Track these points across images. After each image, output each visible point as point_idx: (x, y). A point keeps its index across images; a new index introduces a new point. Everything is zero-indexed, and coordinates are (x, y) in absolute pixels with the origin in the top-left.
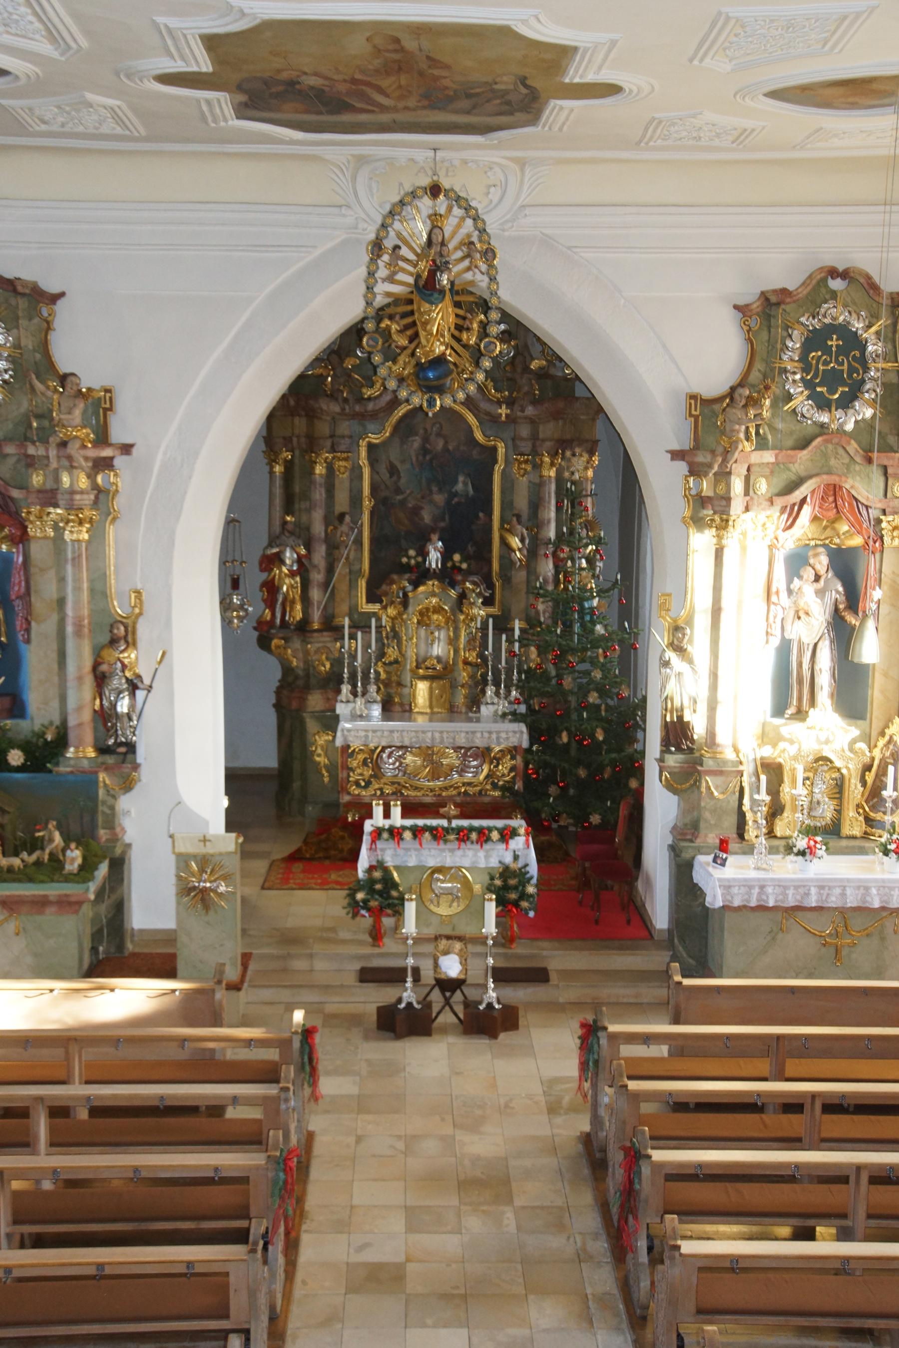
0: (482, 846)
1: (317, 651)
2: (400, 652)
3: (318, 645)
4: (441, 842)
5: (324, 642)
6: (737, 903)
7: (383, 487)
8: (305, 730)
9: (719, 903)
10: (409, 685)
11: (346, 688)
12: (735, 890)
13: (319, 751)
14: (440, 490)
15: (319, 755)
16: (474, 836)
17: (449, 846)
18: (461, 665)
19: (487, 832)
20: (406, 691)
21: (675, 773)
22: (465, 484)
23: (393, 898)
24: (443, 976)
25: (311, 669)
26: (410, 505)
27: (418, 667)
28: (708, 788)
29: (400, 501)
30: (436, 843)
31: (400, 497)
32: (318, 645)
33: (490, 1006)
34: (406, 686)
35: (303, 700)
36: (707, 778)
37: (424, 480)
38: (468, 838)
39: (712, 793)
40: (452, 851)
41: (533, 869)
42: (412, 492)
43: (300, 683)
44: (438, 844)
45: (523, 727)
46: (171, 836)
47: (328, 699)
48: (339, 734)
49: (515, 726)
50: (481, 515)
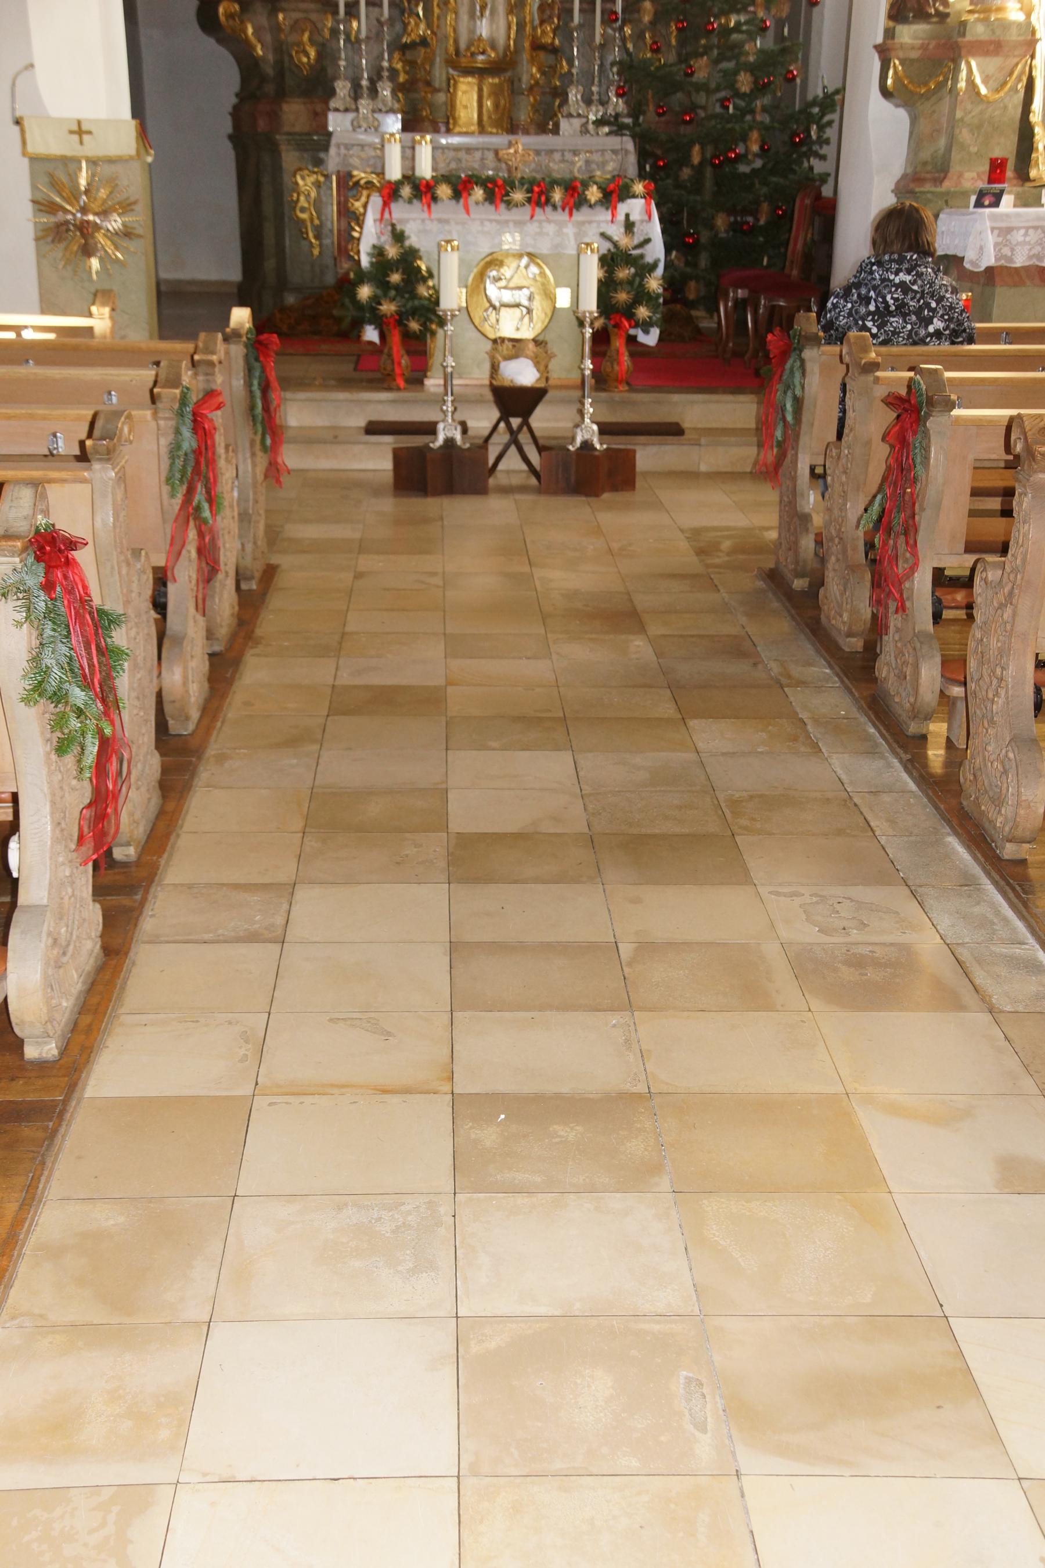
0: (571, 215)
1: (296, 27)
2: (429, 26)
3: (295, 15)
4: (502, 206)
5: (305, 11)
6: (1020, 261)
8: (281, 168)
9: (989, 260)
10: (444, 85)
11: (343, 88)
12: (1018, 236)
13: (303, 202)
15: (303, 210)
16: (557, 196)
17: (517, 214)
18: (525, 56)
19: (580, 189)
20: (441, 97)
21: (912, 61)
23: (421, 298)
24: (507, 384)
25: (286, 59)
27: (457, 52)
28: (970, 82)
30: (492, 208)
32: (295, 15)
33: (587, 445)
34: (439, 90)
35: (274, 116)
36: (973, 63)
38: (548, 201)
39: (978, 93)
40: (519, 224)
41: (656, 251)
43: (270, 88)
44: (496, 207)
45: (629, 144)
46: (18, 122)
47: (316, 114)
48: (333, 151)
49: (615, 142)
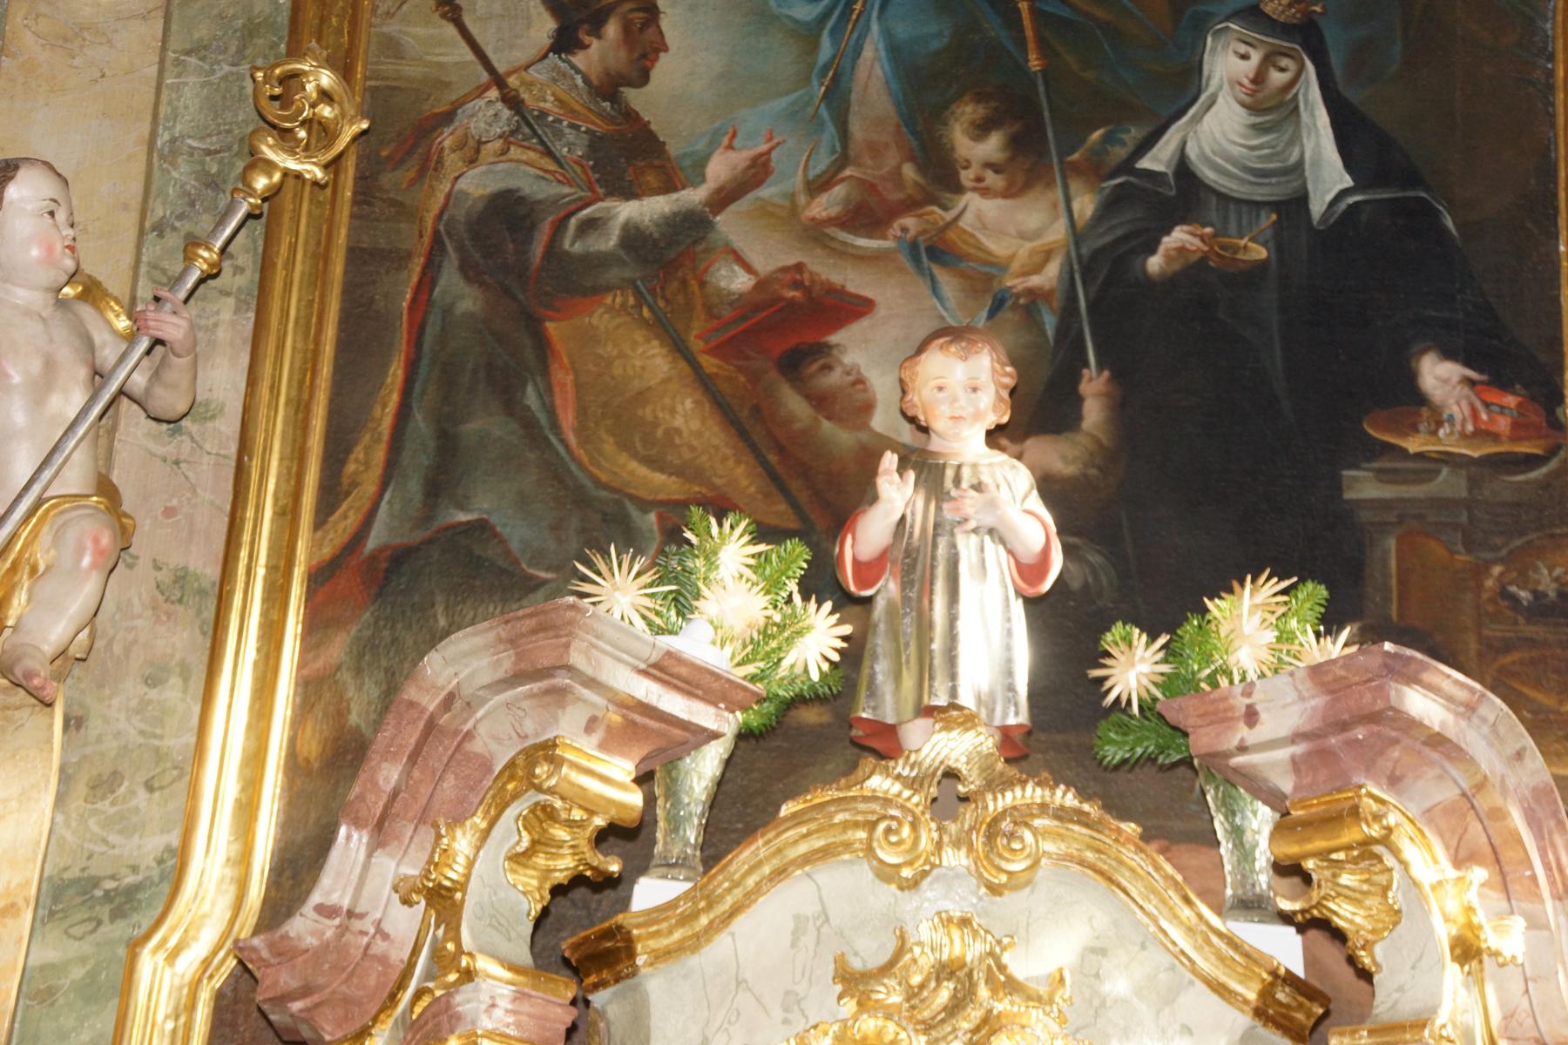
7: (485, 116)
14: (1027, 165)
22: (1271, 109)
26: (739, 282)
29: (634, 238)
31: (647, 210)
37: (872, 70)
42: (758, 171)
50: (1439, 375)
